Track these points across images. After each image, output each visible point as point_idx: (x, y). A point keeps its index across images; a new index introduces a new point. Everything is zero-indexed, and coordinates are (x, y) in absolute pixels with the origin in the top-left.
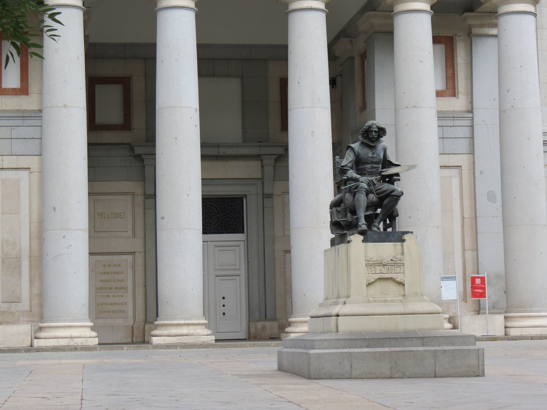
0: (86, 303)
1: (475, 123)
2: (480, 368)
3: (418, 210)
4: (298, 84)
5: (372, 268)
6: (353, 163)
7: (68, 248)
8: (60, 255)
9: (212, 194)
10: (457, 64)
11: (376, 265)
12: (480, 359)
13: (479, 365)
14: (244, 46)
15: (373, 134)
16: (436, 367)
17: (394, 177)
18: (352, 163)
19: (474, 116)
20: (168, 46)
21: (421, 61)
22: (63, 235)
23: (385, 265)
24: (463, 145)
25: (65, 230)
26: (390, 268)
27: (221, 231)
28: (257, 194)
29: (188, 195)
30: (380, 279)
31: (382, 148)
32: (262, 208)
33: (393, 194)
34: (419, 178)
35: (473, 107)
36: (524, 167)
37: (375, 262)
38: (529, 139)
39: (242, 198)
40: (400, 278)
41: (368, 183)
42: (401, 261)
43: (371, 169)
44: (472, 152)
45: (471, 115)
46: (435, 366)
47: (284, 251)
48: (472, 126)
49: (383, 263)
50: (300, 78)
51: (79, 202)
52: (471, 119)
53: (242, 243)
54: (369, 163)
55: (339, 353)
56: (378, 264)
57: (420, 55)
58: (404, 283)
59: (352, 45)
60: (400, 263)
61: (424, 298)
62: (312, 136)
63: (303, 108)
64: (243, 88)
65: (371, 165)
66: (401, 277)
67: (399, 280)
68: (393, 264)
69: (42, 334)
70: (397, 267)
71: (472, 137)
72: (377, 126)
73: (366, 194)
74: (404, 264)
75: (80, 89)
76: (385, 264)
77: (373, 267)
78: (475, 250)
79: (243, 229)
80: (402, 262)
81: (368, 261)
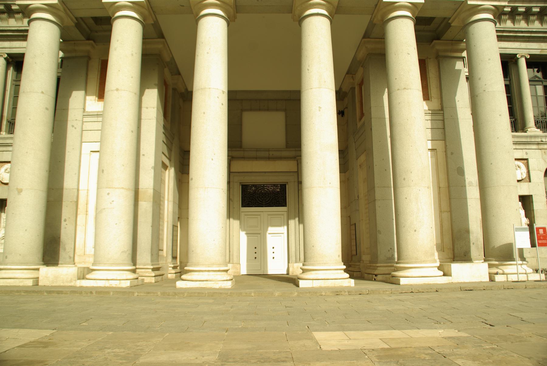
0: (126, 250)
1: (445, 118)
3: (411, 172)
4: (307, 70)
7: (111, 203)
8: (104, 209)
10: (429, 77)
14: (287, 91)
19: (444, 113)
21: (409, 54)
22: (107, 192)
25: (110, 188)
27: (272, 205)
28: (294, 182)
29: (212, 160)
32: (297, 190)
34: (411, 146)
35: (443, 106)
36: (498, 138)
38: (500, 115)
39: (286, 185)
44: (444, 140)
45: (442, 112)
48: (443, 120)
50: (309, 66)
51: (123, 165)
52: (442, 115)
53: (286, 212)
57: (407, 49)
59: (353, 79)
62: (320, 110)
63: (311, 89)
64: (286, 117)
75: (132, 77)
78: (449, 211)
79: (286, 204)
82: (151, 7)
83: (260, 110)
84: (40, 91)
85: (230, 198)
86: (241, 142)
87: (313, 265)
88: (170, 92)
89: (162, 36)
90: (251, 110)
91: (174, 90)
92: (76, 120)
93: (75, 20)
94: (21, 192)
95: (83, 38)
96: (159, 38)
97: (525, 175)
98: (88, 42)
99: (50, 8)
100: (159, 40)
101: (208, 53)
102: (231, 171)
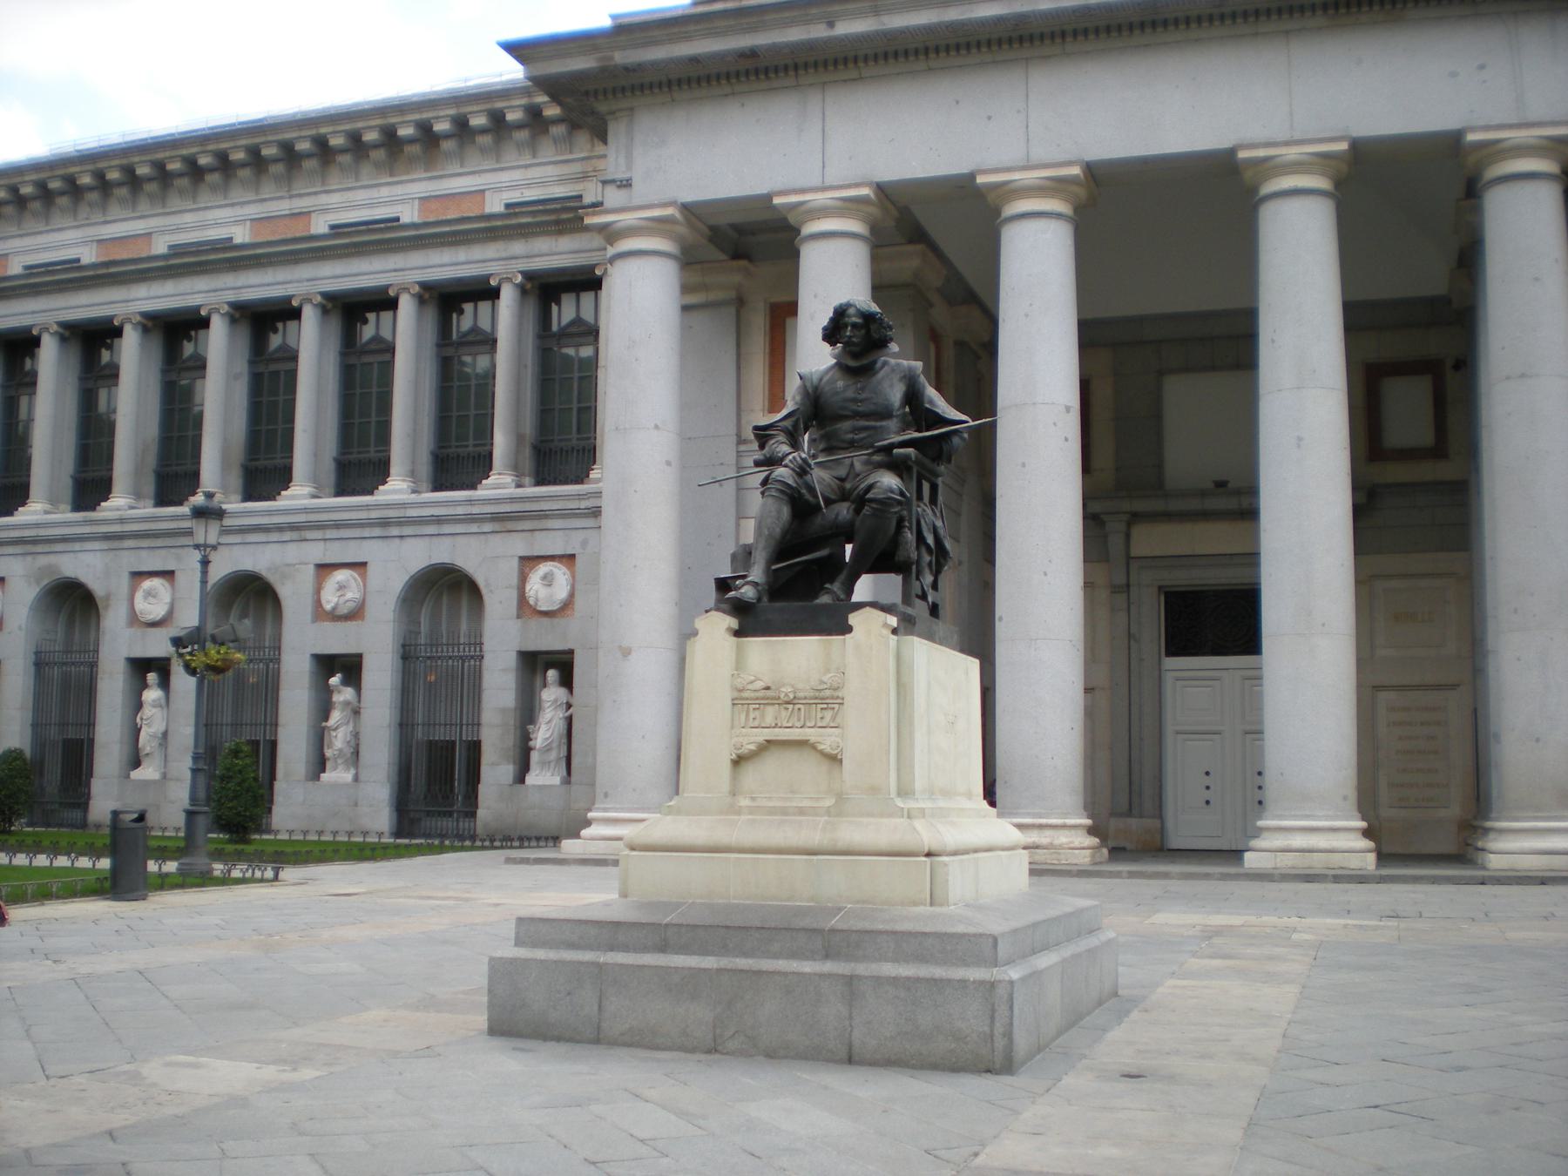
2: (996, 1045)
5: (751, 709)
6: (797, 420)
9: (1234, 581)
11: (762, 702)
12: (996, 1014)
13: (992, 1036)
15: (848, 334)
16: (851, 1031)
17: (895, 451)
18: (794, 419)
20: (1013, 289)
23: (788, 703)
26: (803, 710)
29: (1045, 574)
30: (770, 744)
31: (902, 374)
33: (870, 496)
37: (761, 694)
40: (828, 743)
41: (801, 467)
42: (835, 689)
43: (851, 432)
46: (851, 1026)
47: (1374, 687)
49: (782, 696)
54: (846, 418)
55: (572, 963)
56: (768, 699)
58: (839, 757)
60: (832, 698)
61: (896, 805)
62: (1299, 446)
65: (851, 422)
66: (833, 739)
67: (825, 746)
68: (811, 699)
70: (825, 709)
72: (858, 310)
73: (785, 498)
74: (843, 699)
76: (786, 699)
77: (754, 709)
80: (836, 694)
81: (740, 691)
82: (886, 196)
83: (1214, 368)
84: (653, 425)
85: (1132, 632)
86: (1160, 466)
87: (1281, 817)
88: (949, 354)
89: (915, 234)
90: (1187, 369)
91: (960, 344)
92: (722, 464)
93: (707, 231)
94: (629, 654)
95: (723, 257)
96: (911, 242)
98: (736, 263)
100: (911, 248)
101: (1027, 315)
102: (1132, 555)
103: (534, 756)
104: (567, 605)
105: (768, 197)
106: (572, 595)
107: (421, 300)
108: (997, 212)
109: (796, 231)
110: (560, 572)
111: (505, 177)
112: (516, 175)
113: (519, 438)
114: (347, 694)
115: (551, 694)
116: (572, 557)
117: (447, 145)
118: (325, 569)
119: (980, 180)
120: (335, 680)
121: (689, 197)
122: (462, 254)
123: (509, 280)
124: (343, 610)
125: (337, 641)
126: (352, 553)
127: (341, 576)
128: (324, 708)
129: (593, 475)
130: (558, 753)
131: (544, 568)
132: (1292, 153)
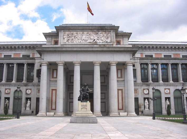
24: (123, 86)
44: (124, 87)
69: (56, 114)
71: (124, 84)
97: (148, 93)
99: (46, 63)
103: (27, 107)
104: (30, 93)
105: (56, 62)
106: (31, 92)
107: (16, 64)
108: (74, 65)
109: (58, 65)
110: (30, 91)
111: (23, 52)
112: (24, 52)
113: (26, 78)
114: (8, 101)
115: (29, 102)
116: (31, 89)
117: (17, 49)
118: (6, 89)
119: (73, 62)
120: (6, 100)
121: (49, 61)
122: (21, 61)
123: (26, 63)
124: (8, 93)
125: (7, 96)
126: (10, 88)
127: (7, 90)
128: (5, 102)
129: (33, 82)
130: (29, 107)
131: (28, 90)
132: (97, 62)
